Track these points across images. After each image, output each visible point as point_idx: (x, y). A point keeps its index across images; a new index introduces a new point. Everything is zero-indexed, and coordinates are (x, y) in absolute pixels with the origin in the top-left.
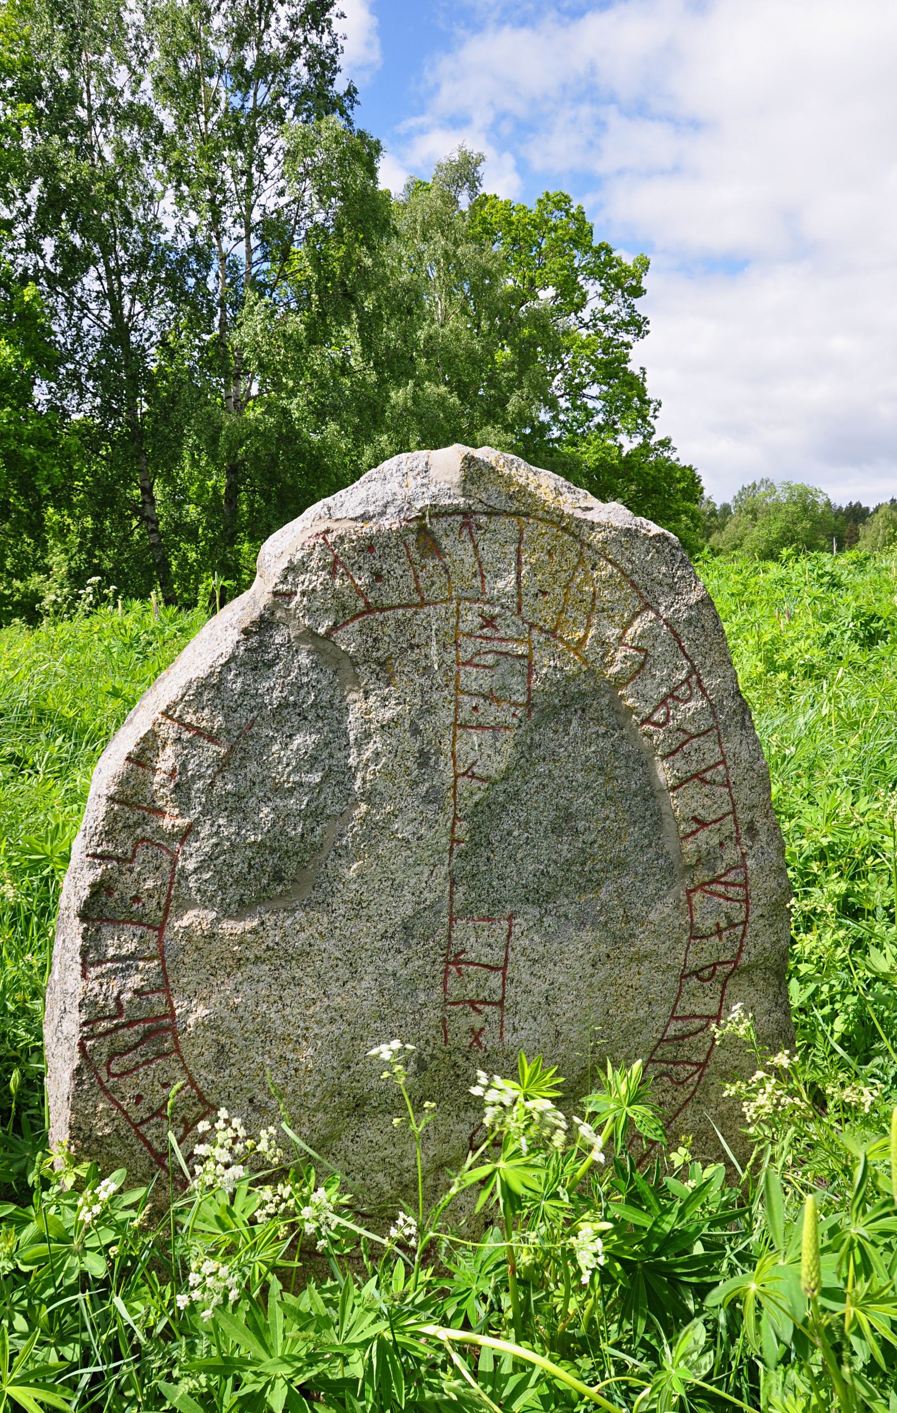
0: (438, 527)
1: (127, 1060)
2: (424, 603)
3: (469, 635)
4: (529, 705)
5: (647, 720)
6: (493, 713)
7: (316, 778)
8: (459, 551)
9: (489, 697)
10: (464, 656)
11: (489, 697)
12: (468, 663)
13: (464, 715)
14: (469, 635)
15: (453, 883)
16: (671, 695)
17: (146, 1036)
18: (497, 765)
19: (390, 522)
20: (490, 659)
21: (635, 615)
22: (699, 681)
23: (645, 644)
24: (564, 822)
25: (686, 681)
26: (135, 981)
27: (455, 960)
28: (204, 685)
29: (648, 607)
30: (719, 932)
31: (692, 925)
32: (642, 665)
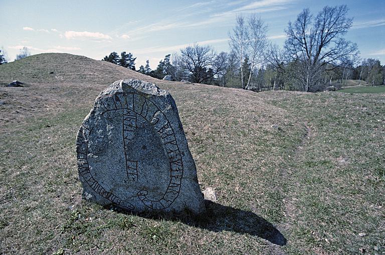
0: (119, 96)
1: (85, 172)
2: (117, 109)
3: (125, 115)
4: (137, 127)
5: (159, 131)
6: (129, 128)
7: (103, 137)
8: (122, 99)
9: (129, 125)
10: (124, 118)
11: (129, 125)
12: (125, 120)
13: (125, 128)
14: (125, 115)
15: (126, 155)
16: (164, 127)
17: (86, 170)
18: (131, 138)
19: (110, 96)
20: (129, 119)
21: (157, 111)
22: (170, 125)
23: (158, 117)
24: (144, 147)
25: (167, 124)
26: (83, 162)
27: (128, 167)
28: (86, 121)
29: (159, 110)
30: (177, 171)
31: (171, 168)
32: (158, 121)
